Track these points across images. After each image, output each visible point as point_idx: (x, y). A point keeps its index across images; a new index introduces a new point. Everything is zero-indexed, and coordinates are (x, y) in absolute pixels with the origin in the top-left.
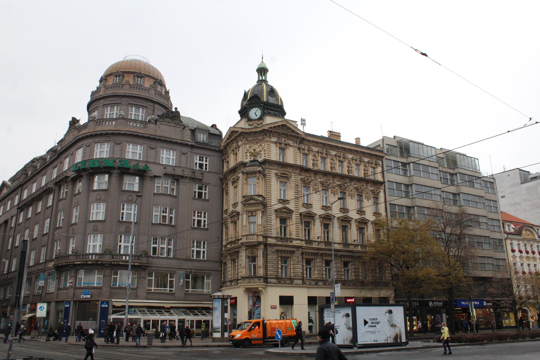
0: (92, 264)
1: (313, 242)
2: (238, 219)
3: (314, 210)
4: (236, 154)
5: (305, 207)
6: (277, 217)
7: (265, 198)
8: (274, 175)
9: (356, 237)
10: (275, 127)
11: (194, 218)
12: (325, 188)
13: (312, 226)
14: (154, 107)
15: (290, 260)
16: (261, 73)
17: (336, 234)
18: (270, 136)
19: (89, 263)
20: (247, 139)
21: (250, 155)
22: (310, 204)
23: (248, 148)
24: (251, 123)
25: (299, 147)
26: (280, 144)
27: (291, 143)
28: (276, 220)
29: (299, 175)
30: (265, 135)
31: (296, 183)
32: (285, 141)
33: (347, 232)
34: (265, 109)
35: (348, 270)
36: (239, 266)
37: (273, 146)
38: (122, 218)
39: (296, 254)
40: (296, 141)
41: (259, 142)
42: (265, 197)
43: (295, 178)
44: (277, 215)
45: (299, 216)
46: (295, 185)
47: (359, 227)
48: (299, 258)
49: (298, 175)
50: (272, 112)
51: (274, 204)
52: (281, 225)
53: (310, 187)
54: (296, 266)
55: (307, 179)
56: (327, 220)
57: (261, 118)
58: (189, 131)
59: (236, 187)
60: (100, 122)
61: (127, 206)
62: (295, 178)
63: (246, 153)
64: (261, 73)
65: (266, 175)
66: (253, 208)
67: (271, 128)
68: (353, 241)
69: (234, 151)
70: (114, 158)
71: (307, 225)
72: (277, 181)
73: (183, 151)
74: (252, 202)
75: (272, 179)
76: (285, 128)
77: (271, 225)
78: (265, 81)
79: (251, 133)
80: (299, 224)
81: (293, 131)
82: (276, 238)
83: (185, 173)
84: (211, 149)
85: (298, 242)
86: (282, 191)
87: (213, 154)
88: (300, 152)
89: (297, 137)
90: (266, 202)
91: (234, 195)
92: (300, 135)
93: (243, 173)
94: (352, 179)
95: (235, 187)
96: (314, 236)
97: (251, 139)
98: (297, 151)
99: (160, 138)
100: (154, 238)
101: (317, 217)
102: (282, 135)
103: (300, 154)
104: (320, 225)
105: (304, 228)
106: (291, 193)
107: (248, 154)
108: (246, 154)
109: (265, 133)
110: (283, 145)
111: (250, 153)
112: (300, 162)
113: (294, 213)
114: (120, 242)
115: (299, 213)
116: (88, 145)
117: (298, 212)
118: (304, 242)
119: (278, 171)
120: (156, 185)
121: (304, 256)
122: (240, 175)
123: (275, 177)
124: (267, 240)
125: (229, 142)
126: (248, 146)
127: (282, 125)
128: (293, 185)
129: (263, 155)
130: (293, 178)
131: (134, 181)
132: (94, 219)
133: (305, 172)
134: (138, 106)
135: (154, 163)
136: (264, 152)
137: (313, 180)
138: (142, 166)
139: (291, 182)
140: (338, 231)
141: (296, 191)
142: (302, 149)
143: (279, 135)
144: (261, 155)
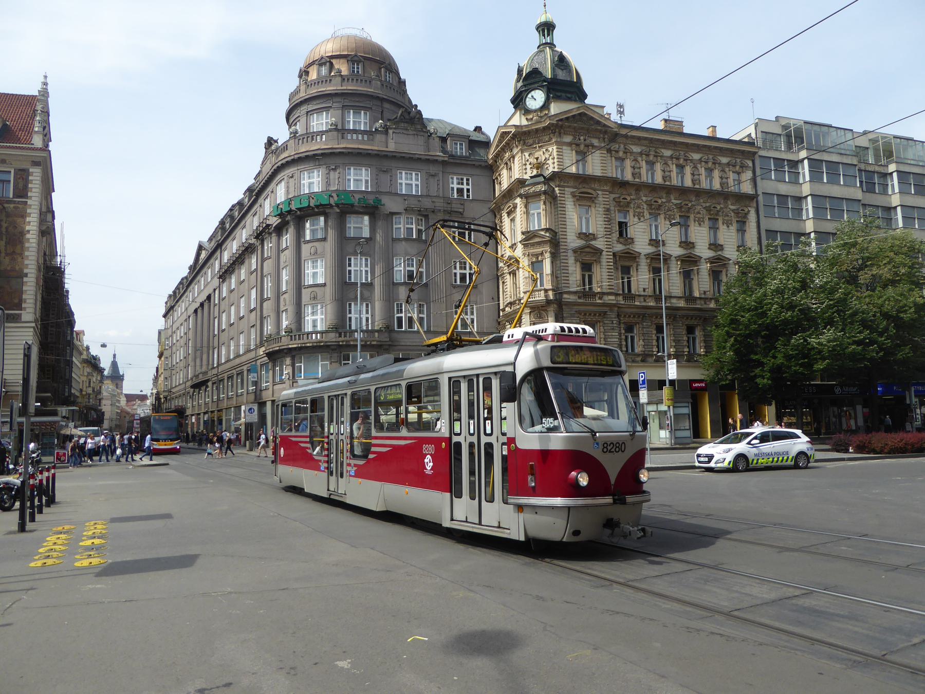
0: (313, 347)
1: (636, 297)
2: (518, 268)
3: (637, 247)
4: (510, 169)
5: (621, 243)
6: (576, 260)
7: (556, 233)
8: (570, 196)
9: (708, 286)
10: (567, 118)
11: (454, 271)
12: (655, 210)
14: (382, 107)
15: (600, 326)
16: (543, 31)
17: (673, 283)
18: (560, 133)
19: (308, 345)
20: (524, 143)
21: (531, 168)
24: (531, 116)
25: (610, 148)
26: (578, 145)
27: (595, 142)
28: (574, 265)
29: (610, 192)
30: (552, 133)
31: (605, 206)
32: (585, 140)
33: (693, 279)
34: (551, 90)
35: (694, 339)
37: (566, 150)
38: (350, 278)
39: (608, 316)
40: (604, 139)
41: (544, 146)
42: (557, 231)
43: (603, 197)
44: (576, 257)
45: (611, 257)
47: (713, 271)
48: (614, 322)
49: (608, 193)
50: (563, 95)
51: (572, 241)
52: (583, 273)
53: (629, 211)
54: (610, 334)
55: (623, 199)
56: (657, 262)
57: (545, 106)
58: (437, 140)
59: (513, 220)
60: (303, 138)
61: (354, 261)
62: (603, 197)
63: (526, 164)
64: (543, 31)
67: (561, 120)
68: (703, 292)
69: (506, 164)
70: (329, 191)
71: (626, 270)
72: (575, 205)
73: (431, 172)
74: (537, 240)
75: (567, 203)
76: (585, 118)
77: (568, 273)
78: (551, 45)
79: (529, 132)
80: (612, 271)
81: (598, 123)
83: (437, 204)
85: (613, 297)
86: (584, 220)
87: (477, 172)
89: (606, 132)
91: (511, 231)
92: (610, 127)
93: (521, 196)
94: (699, 193)
95: (511, 220)
96: (638, 288)
97: (531, 141)
98: (605, 155)
99: (394, 154)
100: (397, 304)
101: (642, 257)
102: (580, 131)
103: (611, 160)
104: (647, 270)
105: (620, 276)
106: (598, 223)
107: (528, 167)
108: (524, 167)
109: (552, 130)
110: (582, 147)
111: (530, 164)
112: (612, 173)
113: (604, 253)
114: (350, 313)
115: (611, 254)
116: (291, 175)
118: (620, 298)
119: (576, 190)
120: (394, 226)
121: (622, 319)
122: (518, 201)
123: (571, 200)
124: (562, 296)
125: (499, 151)
126: (527, 154)
127: (580, 114)
128: (600, 209)
129: (552, 166)
130: (601, 199)
131: (362, 223)
132: (311, 283)
133: (620, 187)
134: (357, 109)
135: (389, 193)
137: (634, 199)
138: (371, 200)
139: (597, 205)
140: (678, 278)
141: (606, 219)
142: (616, 151)
143: (576, 132)
144: (548, 166)
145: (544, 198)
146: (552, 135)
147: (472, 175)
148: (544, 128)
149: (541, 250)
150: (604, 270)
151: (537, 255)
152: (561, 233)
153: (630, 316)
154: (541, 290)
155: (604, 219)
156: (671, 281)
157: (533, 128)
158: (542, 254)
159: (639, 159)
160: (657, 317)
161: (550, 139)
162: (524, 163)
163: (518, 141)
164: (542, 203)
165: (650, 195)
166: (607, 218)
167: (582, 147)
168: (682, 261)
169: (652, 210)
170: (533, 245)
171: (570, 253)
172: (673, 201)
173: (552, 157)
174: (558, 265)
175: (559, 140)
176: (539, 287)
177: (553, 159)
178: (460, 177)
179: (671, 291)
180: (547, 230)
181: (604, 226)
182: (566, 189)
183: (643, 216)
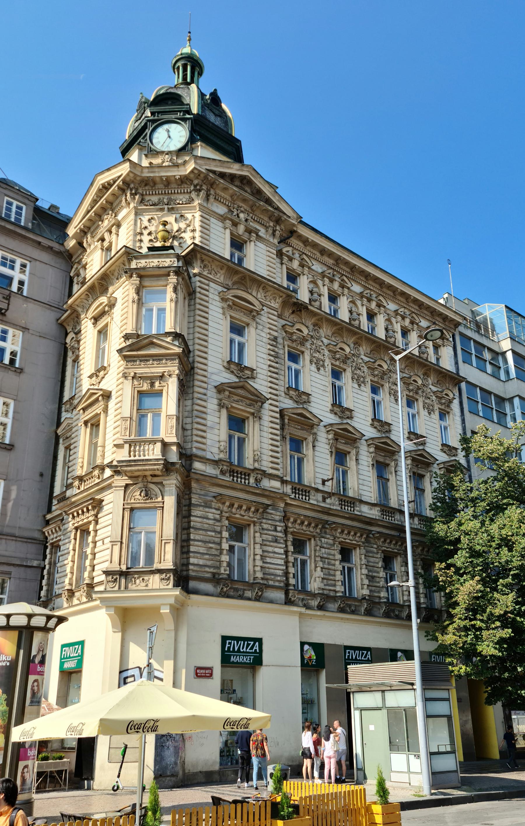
1: (312, 492)
2: (106, 410)
5: (291, 398)
6: (221, 406)
8: (217, 298)
13: (307, 450)
15: (255, 532)
20: (143, 199)
22: (304, 393)
23: (146, 223)
26: (235, 224)
28: (217, 414)
30: (196, 190)
32: (246, 220)
36: (98, 544)
37: (216, 225)
39: (269, 517)
40: (274, 231)
44: (220, 400)
45: (278, 415)
46: (268, 336)
48: (279, 529)
54: (270, 549)
55: (298, 330)
59: (103, 333)
63: (141, 234)
65: (194, 292)
66: (157, 370)
67: (214, 172)
69: (103, 240)
72: (224, 314)
77: (205, 425)
82: (216, 463)
84: (39, 243)
87: (45, 256)
88: (282, 264)
90: (194, 362)
92: (285, 214)
95: (100, 332)
97: (155, 199)
103: (282, 269)
108: (138, 237)
109: (195, 186)
110: (241, 229)
113: (266, 406)
115: (278, 410)
117: (277, 407)
118: (288, 489)
121: (290, 525)
125: (90, 220)
128: (264, 335)
130: (264, 319)
136: (191, 234)
139: (260, 327)
140: (370, 474)
141: (272, 353)
142: (288, 256)
145: (175, 281)
146: (193, 195)
147: (32, 259)
148: (184, 180)
149: (161, 370)
150: (265, 434)
151: (152, 379)
152: (197, 353)
153: (302, 523)
154: (154, 442)
155: (268, 352)
156: (361, 477)
157: (163, 174)
158: (162, 377)
159: (320, 283)
160: (342, 532)
161: (191, 200)
162: (138, 230)
163: (131, 194)
164: (170, 289)
165: (333, 339)
166: (273, 351)
167: (241, 229)
168: (377, 448)
169: (336, 360)
170: (145, 358)
171: (212, 393)
172: (363, 357)
173: (191, 228)
174: (189, 408)
175: (205, 205)
176: (149, 435)
177: (194, 231)
178: (10, 256)
179: (361, 492)
180: (177, 336)
181: (269, 363)
182: (212, 284)
183: (323, 366)
